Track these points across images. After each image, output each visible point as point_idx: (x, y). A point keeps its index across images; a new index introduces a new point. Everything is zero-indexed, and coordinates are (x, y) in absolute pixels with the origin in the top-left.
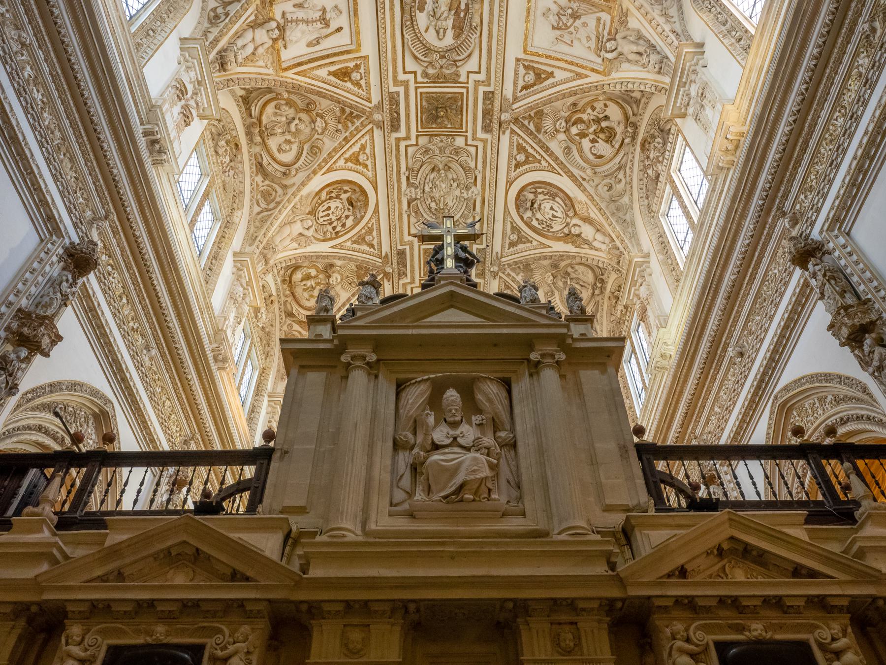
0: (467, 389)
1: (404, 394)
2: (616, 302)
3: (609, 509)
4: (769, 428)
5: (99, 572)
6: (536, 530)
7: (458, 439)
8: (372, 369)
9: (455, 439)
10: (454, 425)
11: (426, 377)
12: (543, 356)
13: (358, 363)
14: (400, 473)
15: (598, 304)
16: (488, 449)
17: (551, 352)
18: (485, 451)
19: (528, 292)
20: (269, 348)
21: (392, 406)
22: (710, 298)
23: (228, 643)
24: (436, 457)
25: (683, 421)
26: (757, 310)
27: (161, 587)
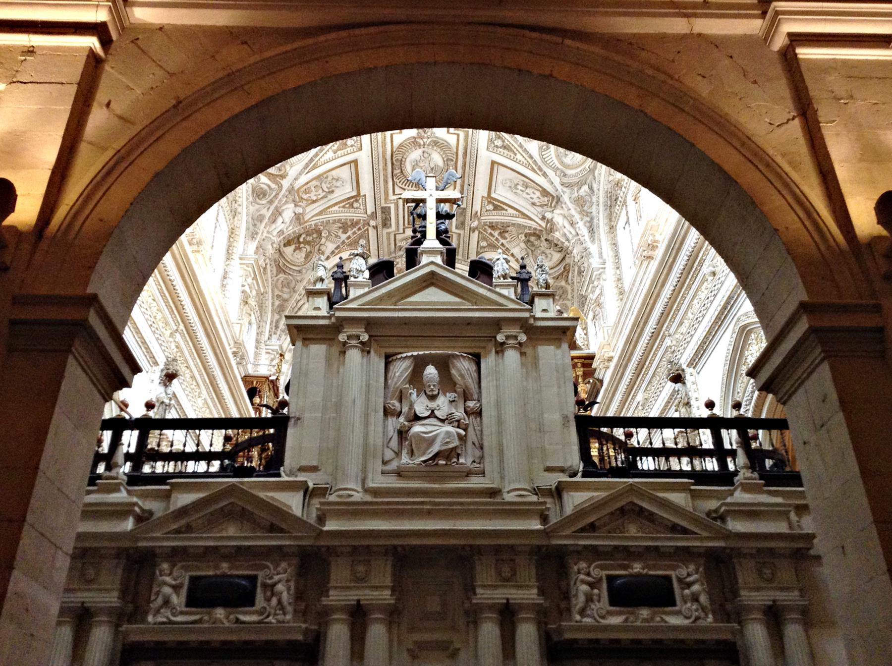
0: (443, 364)
1: (391, 368)
3: (549, 469)
5: (175, 526)
6: (492, 488)
8: (365, 348)
9: (433, 411)
10: (432, 398)
11: (409, 354)
12: (507, 337)
13: (354, 342)
16: (458, 421)
17: (514, 334)
18: (456, 424)
19: (500, 267)
20: (236, 205)
21: (382, 379)
23: (274, 574)
24: (417, 428)
25: (659, 320)
27: (221, 538)
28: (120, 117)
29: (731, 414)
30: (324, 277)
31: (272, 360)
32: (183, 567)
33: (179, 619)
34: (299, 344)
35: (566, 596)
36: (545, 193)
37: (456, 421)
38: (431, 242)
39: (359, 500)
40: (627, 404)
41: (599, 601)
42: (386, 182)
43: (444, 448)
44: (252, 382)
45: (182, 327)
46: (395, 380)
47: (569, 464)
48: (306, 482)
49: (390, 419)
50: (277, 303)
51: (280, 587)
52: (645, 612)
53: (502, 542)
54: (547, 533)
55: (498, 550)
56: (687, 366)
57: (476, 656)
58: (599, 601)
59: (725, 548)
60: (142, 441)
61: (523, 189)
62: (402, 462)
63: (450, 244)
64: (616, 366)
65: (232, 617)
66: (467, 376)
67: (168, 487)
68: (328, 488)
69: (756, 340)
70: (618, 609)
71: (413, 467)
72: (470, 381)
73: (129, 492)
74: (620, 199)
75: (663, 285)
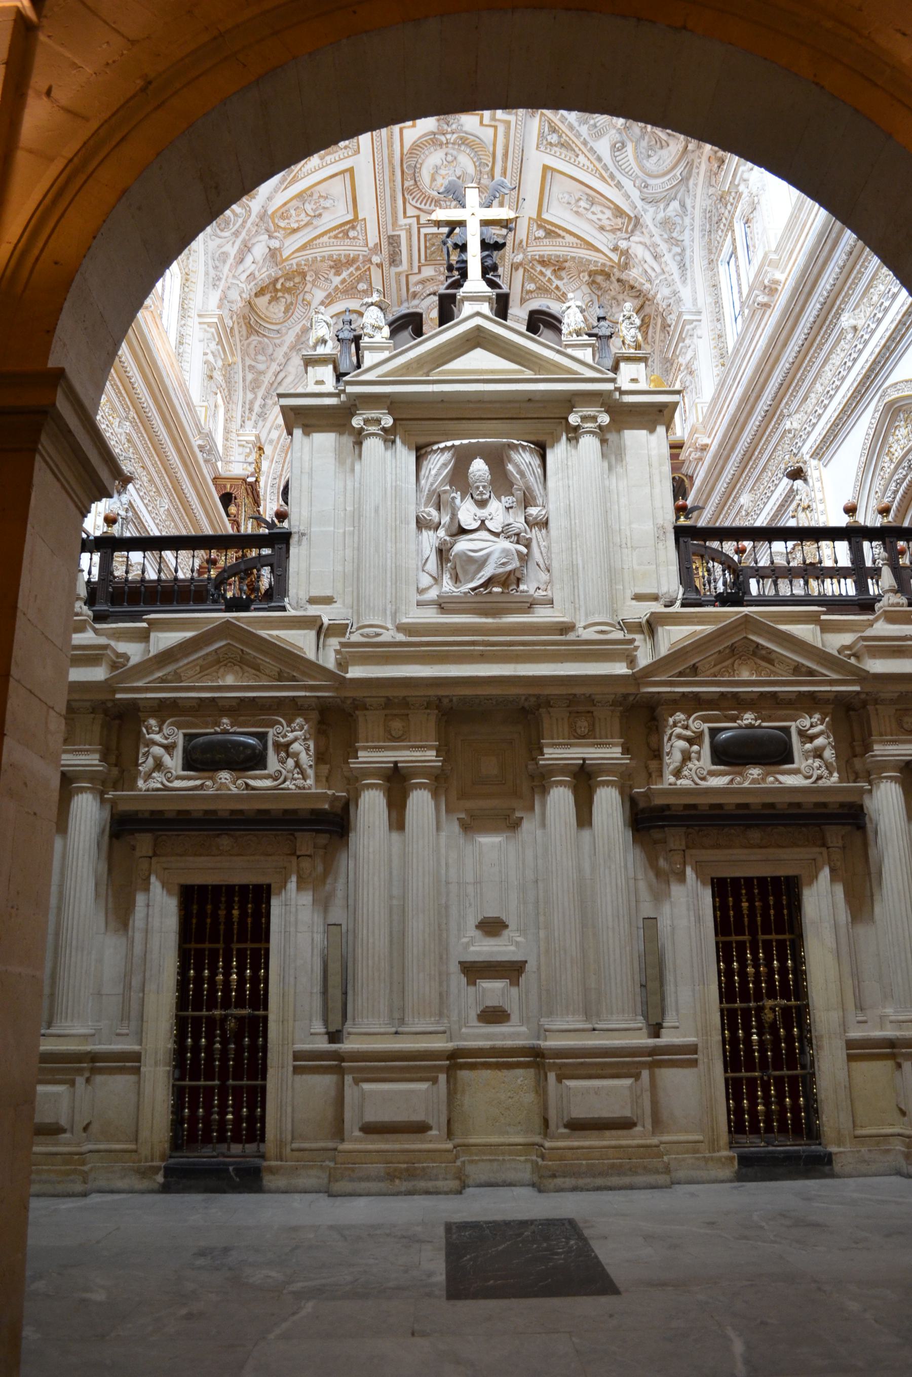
2: (719, 167)
3: (638, 597)
4: (869, 427)
6: (563, 623)
7: (487, 522)
8: (388, 436)
9: (483, 522)
10: (482, 504)
11: (449, 444)
12: (584, 419)
13: (373, 429)
14: (426, 557)
15: (692, 165)
16: (518, 535)
17: (592, 414)
18: (514, 539)
22: (827, 248)
24: (463, 545)
25: (777, 393)
26: (882, 277)
28: (68, 111)
29: (877, 521)
30: (327, 337)
31: (248, 455)
32: (172, 724)
33: (177, 784)
34: (298, 432)
35: (657, 754)
36: (619, 212)
37: (515, 534)
38: (475, 283)
39: (389, 639)
40: (726, 508)
41: (699, 760)
42: (394, 198)
43: (501, 570)
44: (225, 486)
45: (132, 413)
46: (431, 479)
47: (664, 590)
48: (320, 616)
49: (425, 533)
50: (250, 377)
51: (296, 747)
52: (755, 772)
53: (578, 691)
54: (636, 679)
55: (572, 701)
56: (811, 457)
57: (543, 825)
58: (699, 760)
59: (858, 693)
60: (106, 566)
61: (588, 207)
62: (444, 589)
63: (500, 287)
64: (715, 456)
65: (239, 782)
66: (528, 474)
67: (145, 625)
68: (347, 624)
69: (906, 421)
70: (722, 768)
71: (458, 597)
72: (532, 479)
73: (96, 631)
74: (724, 220)
75: (785, 345)
